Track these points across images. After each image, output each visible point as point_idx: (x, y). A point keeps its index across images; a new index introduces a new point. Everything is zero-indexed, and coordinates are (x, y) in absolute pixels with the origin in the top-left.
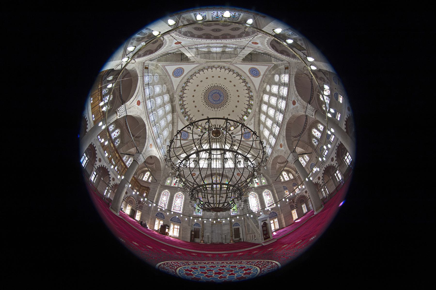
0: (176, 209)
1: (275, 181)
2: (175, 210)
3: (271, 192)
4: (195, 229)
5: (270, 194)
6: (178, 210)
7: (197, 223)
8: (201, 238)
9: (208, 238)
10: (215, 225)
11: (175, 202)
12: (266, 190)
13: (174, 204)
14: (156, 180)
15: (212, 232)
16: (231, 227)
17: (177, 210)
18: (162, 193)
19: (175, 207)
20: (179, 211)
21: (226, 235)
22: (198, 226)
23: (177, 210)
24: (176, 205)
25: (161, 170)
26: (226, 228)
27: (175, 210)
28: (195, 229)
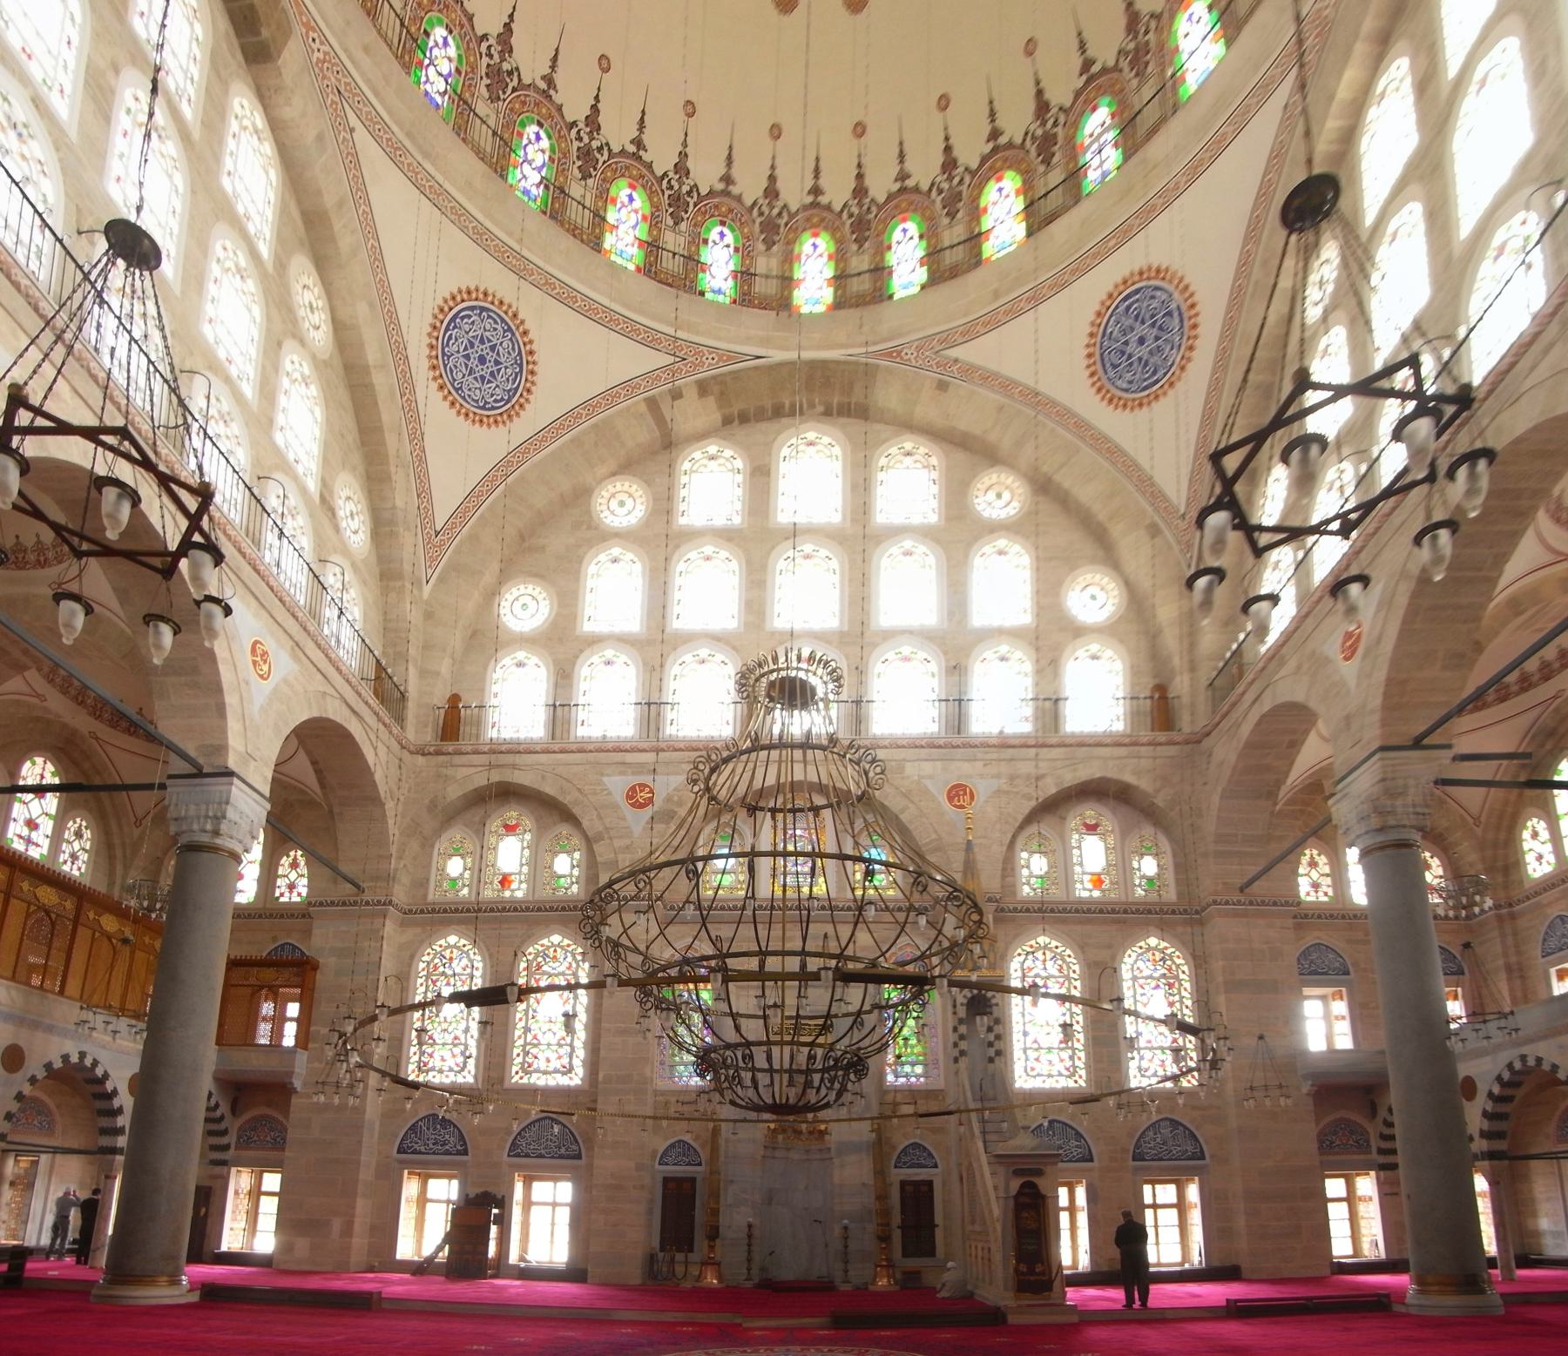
0: (543, 1066)
1: (1242, 890)
2: (537, 1071)
3: (1185, 968)
4: (666, 1180)
5: (1177, 977)
6: (556, 1071)
7: (679, 1141)
8: (706, 1249)
9: (749, 1245)
10: (788, 1149)
11: (531, 1012)
12: (1153, 941)
13: (527, 1029)
14: (350, 886)
15: (769, 1198)
16: (880, 1173)
17: (545, 1073)
18: (422, 965)
19: (534, 1051)
20: (564, 1074)
21: (846, 1228)
22: (689, 1164)
23: (545, 1073)
24: (535, 1037)
25: (375, 800)
26: (854, 1172)
27: (537, 1071)
28: (666, 1180)
